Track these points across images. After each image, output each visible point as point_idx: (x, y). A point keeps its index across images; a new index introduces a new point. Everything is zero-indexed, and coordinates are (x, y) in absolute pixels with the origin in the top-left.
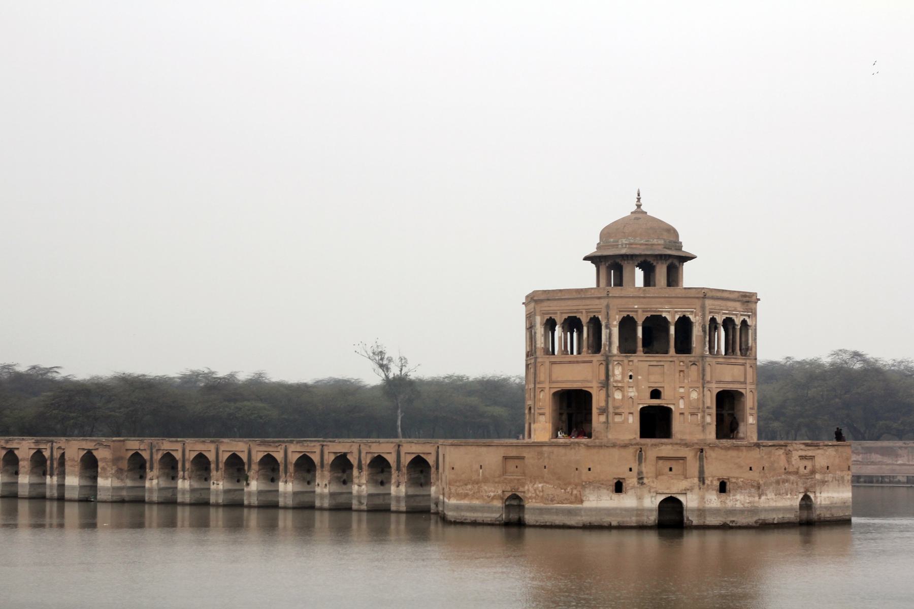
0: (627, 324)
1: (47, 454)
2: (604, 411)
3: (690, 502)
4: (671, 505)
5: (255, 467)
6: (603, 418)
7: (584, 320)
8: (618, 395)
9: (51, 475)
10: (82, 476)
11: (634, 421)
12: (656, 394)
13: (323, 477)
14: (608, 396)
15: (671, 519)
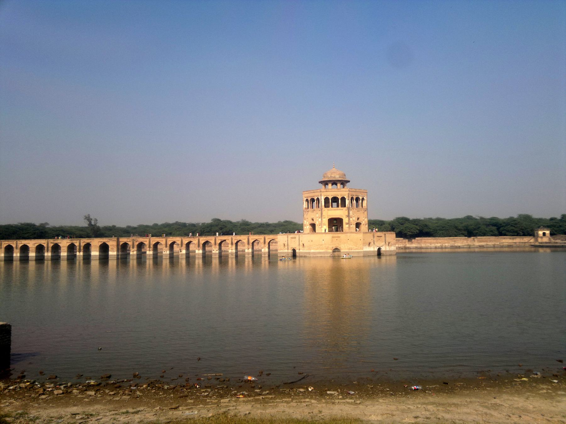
0: (352, 199)
1: (77, 244)
2: (347, 224)
3: (383, 249)
4: (379, 249)
5: (184, 246)
6: (347, 226)
7: (340, 197)
8: (351, 219)
9: (80, 252)
10: (100, 252)
11: (354, 226)
12: (358, 219)
13: (215, 248)
14: (349, 219)
15: (379, 253)
